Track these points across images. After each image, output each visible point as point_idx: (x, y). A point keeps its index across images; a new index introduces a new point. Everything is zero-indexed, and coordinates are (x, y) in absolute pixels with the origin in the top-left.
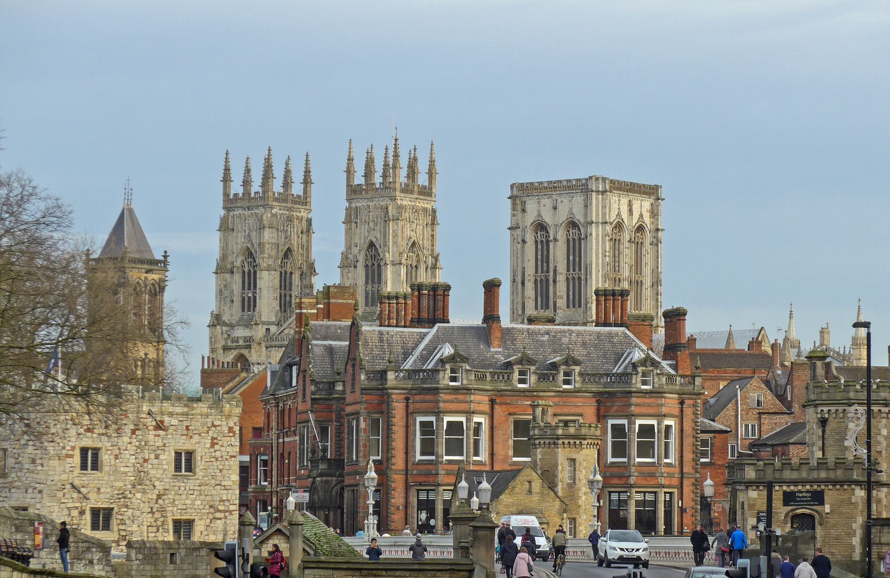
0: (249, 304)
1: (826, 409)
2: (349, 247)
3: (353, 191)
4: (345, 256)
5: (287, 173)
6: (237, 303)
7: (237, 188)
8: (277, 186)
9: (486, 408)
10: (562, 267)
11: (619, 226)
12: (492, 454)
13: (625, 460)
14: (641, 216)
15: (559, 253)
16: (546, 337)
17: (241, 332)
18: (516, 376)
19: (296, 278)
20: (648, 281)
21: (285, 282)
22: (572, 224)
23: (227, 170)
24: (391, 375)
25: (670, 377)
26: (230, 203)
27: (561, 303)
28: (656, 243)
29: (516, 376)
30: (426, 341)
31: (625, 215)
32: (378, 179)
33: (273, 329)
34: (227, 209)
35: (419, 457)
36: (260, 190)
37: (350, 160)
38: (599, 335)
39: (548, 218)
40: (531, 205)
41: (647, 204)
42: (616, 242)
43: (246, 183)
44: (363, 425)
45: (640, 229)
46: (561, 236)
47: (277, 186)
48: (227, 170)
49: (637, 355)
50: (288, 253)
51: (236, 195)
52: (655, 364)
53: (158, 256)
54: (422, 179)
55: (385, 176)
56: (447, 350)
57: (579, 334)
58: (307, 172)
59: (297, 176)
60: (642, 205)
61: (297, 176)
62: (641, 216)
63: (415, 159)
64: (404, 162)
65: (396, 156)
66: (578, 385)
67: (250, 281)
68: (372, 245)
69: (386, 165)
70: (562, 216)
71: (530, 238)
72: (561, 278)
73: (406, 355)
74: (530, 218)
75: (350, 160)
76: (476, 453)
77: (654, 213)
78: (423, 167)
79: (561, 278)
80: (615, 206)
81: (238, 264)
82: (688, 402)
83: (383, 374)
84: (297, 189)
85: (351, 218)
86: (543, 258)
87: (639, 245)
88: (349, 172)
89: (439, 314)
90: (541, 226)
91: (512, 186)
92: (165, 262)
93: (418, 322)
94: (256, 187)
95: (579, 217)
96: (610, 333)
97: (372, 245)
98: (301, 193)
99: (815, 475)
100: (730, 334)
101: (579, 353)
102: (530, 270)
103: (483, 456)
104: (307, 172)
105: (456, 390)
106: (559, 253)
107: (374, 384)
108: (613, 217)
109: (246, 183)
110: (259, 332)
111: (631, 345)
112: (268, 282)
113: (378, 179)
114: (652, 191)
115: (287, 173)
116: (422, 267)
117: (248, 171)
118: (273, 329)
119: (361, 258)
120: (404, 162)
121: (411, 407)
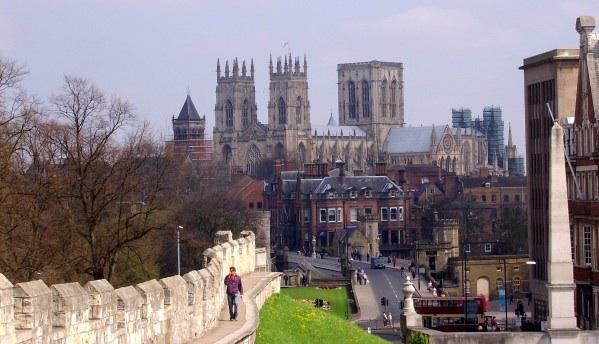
0: (230, 123)
2: (271, 99)
3: (273, 76)
4: (270, 103)
5: (244, 68)
6: (225, 124)
7: (223, 74)
8: (240, 74)
10: (360, 99)
11: (385, 81)
15: (359, 93)
17: (226, 135)
19: (249, 111)
20: (398, 104)
21: (245, 114)
22: (365, 82)
23: (218, 67)
26: (220, 80)
27: (361, 115)
28: (401, 88)
33: (240, 133)
34: (219, 83)
39: (354, 79)
40: (347, 74)
41: (396, 72)
42: (383, 89)
45: (394, 82)
46: (360, 87)
47: (240, 74)
48: (218, 67)
49: (390, 186)
53: (201, 117)
54: (302, 70)
55: (286, 68)
56: (329, 187)
58: (252, 67)
59: (248, 68)
60: (394, 73)
61: (248, 68)
64: (293, 63)
65: (290, 61)
67: (230, 113)
68: (281, 98)
70: (360, 78)
72: (360, 105)
74: (346, 79)
77: (400, 75)
78: (301, 64)
79: (360, 105)
84: (248, 74)
85: (273, 87)
86: (353, 96)
87: (393, 89)
88: (271, 68)
90: (351, 83)
92: (204, 119)
93: (318, 176)
94: (231, 74)
95: (367, 78)
97: (281, 98)
100: (433, 131)
101: (371, 185)
102: (347, 101)
104: (252, 67)
106: (359, 93)
108: (382, 78)
109: (227, 72)
110: (235, 135)
112: (237, 115)
114: (399, 66)
115: (244, 68)
116: (302, 108)
117: (227, 67)
118: (240, 133)
120: (293, 63)
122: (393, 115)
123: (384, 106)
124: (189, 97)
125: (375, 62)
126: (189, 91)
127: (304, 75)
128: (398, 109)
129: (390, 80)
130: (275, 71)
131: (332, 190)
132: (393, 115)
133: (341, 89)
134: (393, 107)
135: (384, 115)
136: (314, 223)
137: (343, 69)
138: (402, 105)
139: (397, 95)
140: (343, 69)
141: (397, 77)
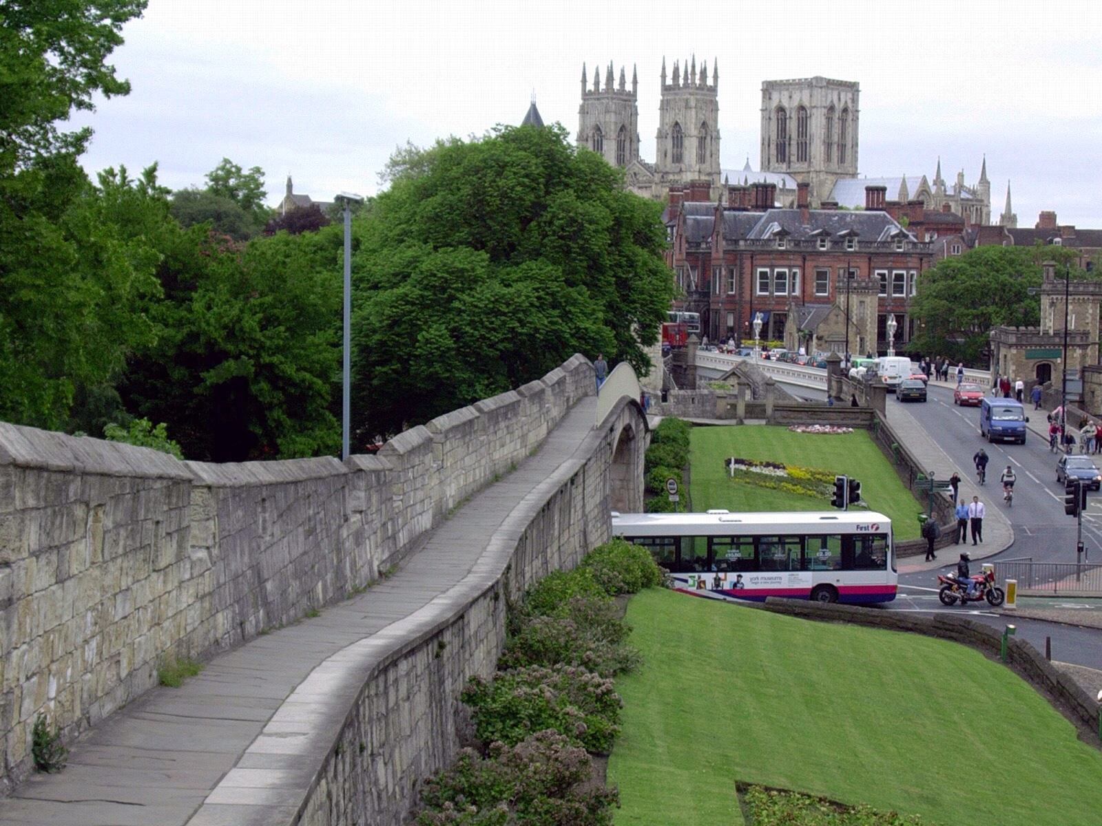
1: (1055, 297)
3: (666, 89)
4: (660, 131)
5: (623, 76)
7: (590, 86)
8: (616, 86)
9: (800, 263)
10: (794, 135)
11: (832, 108)
12: (803, 291)
13: (885, 295)
14: (846, 102)
15: (792, 126)
16: (836, 218)
18: (819, 243)
19: (627, 144)
20: (849, 145)
22: (802, 108)
24: (742, 243)
25: (914, 244)
26: (586, 95)
27: (794, 158)
28: (856, 119)
29: (819, 243)
30: (763, 220)
31: (836, 102)
32: (681, 82)
34: (584, 99)
35: (759, 293)
36: (604, 87)
37: (664, 68)
38: (869, 216)
39: (785, 104)
40: (775, 96)
41: (850, 95)
42: (829, 120)
43: (597, 83)
44: (724, 273)
45: (845, 110)
46: (794, 116)
47: (616, 86)
49: (894, 232)
50: (623, 128)
51: (590, 91)
52: (906, 236)
55: (686, 78)
56: (776, 228)
57: (856, 215)
60: (846, 97)
62: (846, 102)
63: (705, 69)
64: (698, 71)
65: (693, 67)
66: (857, 249)
68: (677, 124)
69: (686, 72)
70: (796, 103)
71: (774, 116)
72: (794, 143)
73: (751, 228)
74: (774, 103)
75: (664, 68)
76: (794, 291)
77: (855, 100)
78: (710, 73)
79: (794, 143)
80: (830, 96)
81: (590, 135)
82: (925, 260)
83: (736, 242)
84: (629, 87)
85: (665, 106)
86: (782, 130)
87: (843, 121)
88: (664, 77)
89: (769, 202)
90: (781, 109)
91: (763, 83)
93: (756, 207)
94: (602, 86)
95: (806, 103)
96: (876, 216)
98: (631, 89)
99: (1051, 341)
100: (904, 180)
102: (774, 137)
103: (797, 293)
105: (782, 252)
106: (792, 126)
107: (731, 248)
109: (597, 83)
111: (888, 223)
113: (681, 82)
114: (853, 87)
115: (623, 76)
116: (709, 138)
117: (597, 75)
119: (670, 132)
120: (698, 71)
121: (755, 262)
122: (842, 160)
123: (829, 145)
124: (534, 107)
125: (818, 79)
126: (534, 96)
127: (713, 90)
128: (849, 152)
129: (839, 107)
130: (669, 82)
131: (782, 234)
132: (842, 160)
133: (766, 119)
134: (842, 147)
135: (828, 158)
136: (747, 297)
137: (769, 88)
138: (855, 145)
139: (849, 130)
140: (769, 88)
141: (850, 105)
